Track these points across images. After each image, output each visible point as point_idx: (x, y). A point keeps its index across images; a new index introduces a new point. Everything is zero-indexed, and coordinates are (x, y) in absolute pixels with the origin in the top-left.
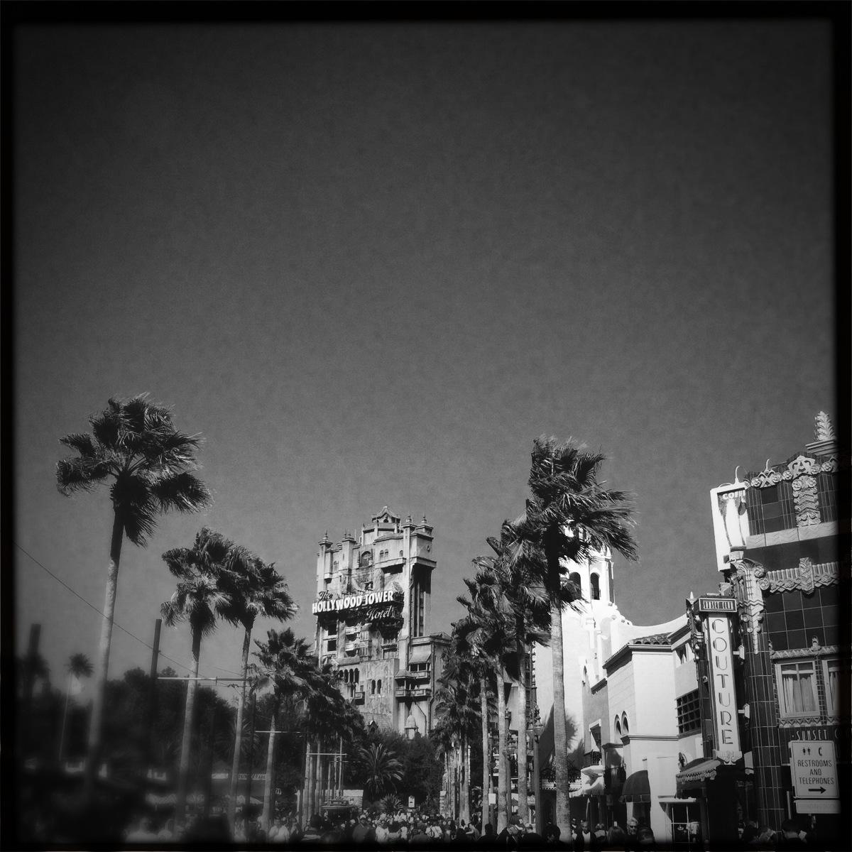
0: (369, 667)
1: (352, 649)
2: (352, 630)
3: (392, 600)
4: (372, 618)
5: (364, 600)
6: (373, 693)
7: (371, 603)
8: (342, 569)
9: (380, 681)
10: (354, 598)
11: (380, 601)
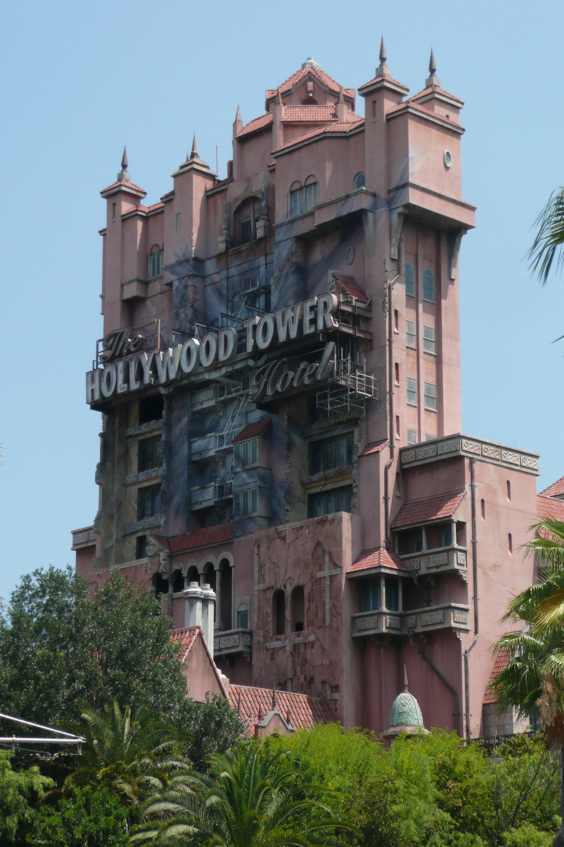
1: (212, 503)
4: (269, 392)
5: (241, 336)
6: (279, 630)
7: (263, 345)
8: (173, 260)
9: (298, 591)
10: (211, 338)
11: (293, 334)
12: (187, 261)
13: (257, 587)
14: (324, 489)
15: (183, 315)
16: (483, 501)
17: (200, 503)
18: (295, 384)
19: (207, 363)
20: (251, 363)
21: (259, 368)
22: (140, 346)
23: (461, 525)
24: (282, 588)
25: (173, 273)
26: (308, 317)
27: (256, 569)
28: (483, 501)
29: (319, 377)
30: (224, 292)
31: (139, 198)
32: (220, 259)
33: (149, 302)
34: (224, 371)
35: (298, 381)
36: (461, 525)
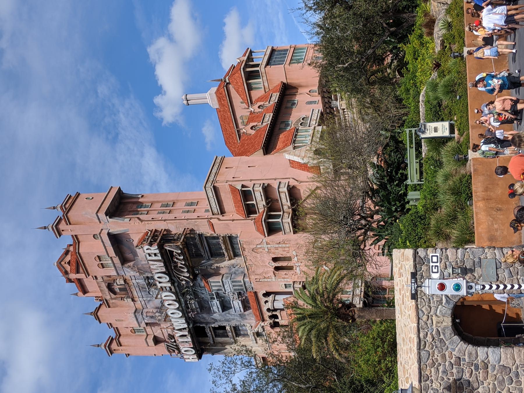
0: (257, 277)
2: (216, 304)
3: (156, 247)
6: (290, 268)
8: (136, 322)
10: (166, 303)
12: (136, 316)
13: (274, 280)
14: (231, 250)
15: (159, 318)
16: (233, 178)
17: (240, 308)
18: (183, 263)
19: (177, 305)
20: (176, 284)
21: (178, 281)
22: (172, 337)
23: (243, 186)
24: (274, 267)
25: (142, 322)
26: (154, 258)
27: (266, 280)
28: (233, 178)
29: (180, 252)
30: (149, 299)
31: (112, 339)
32: (135, 301)
33: (155, 334)
34: (180, 297)
35: (181, 261)
36: (243, 186)
